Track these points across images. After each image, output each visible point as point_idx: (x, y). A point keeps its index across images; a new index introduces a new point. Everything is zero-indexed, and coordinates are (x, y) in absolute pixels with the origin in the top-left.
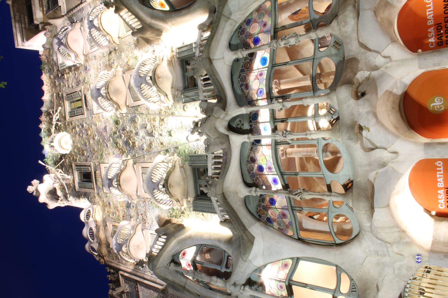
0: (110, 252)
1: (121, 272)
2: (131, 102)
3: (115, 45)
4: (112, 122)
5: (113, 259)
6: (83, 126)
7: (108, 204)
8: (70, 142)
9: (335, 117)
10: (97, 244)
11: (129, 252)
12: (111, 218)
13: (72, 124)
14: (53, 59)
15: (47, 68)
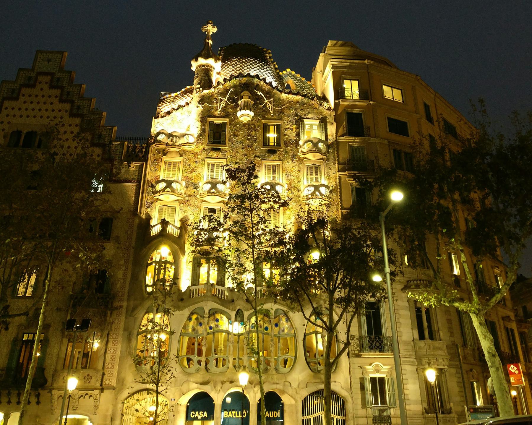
0: (159, 153)
8: (245, 122)
14: (309, 113)
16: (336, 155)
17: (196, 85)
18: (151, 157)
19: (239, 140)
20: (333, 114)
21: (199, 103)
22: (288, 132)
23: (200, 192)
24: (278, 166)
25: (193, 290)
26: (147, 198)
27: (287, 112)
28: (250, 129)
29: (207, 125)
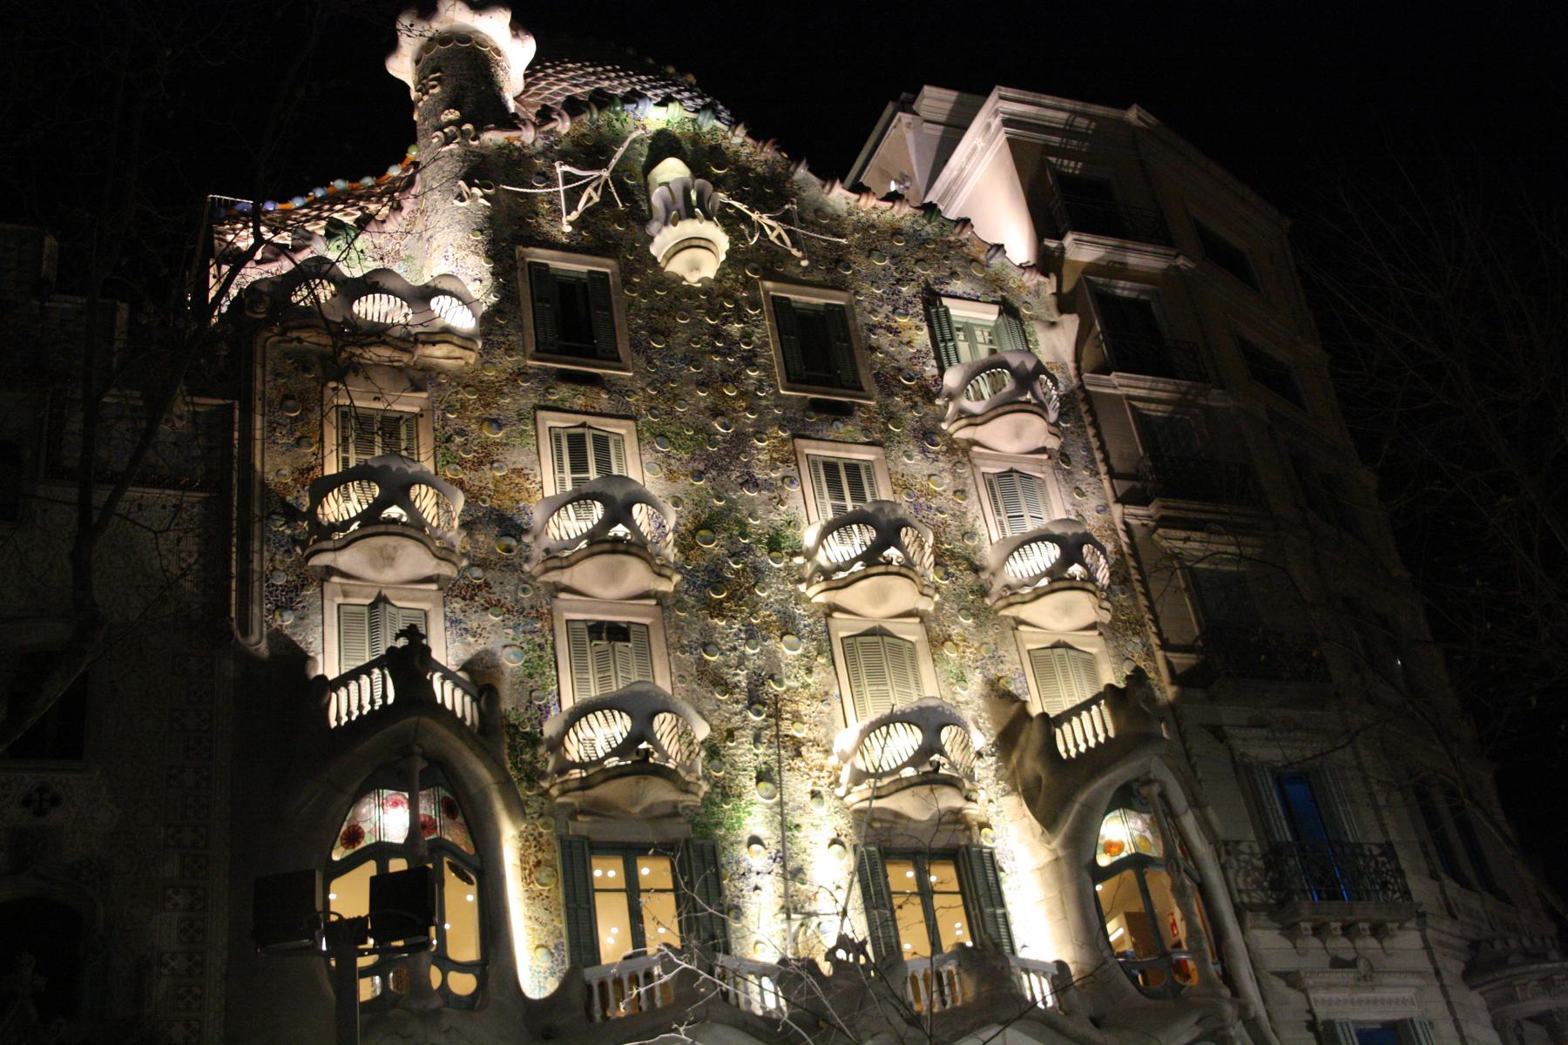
0: (306, 370)
2: (842, 627)
3: (1001, 603)
4: (775, 518)
6: (749, 360)
7: (494, 413)
8: (693, 279)
10: (339, 320)
11: (382, 528)
12: (445, 419)
13: (754, 306)
14: (953, 274)
15: (928, 228)
16: (1095, 443)
19: (679, 352)
20: (1049, 286)
22: (883, 339)
24: (869, 466)
26: (268, 565)
27: (861, 264)
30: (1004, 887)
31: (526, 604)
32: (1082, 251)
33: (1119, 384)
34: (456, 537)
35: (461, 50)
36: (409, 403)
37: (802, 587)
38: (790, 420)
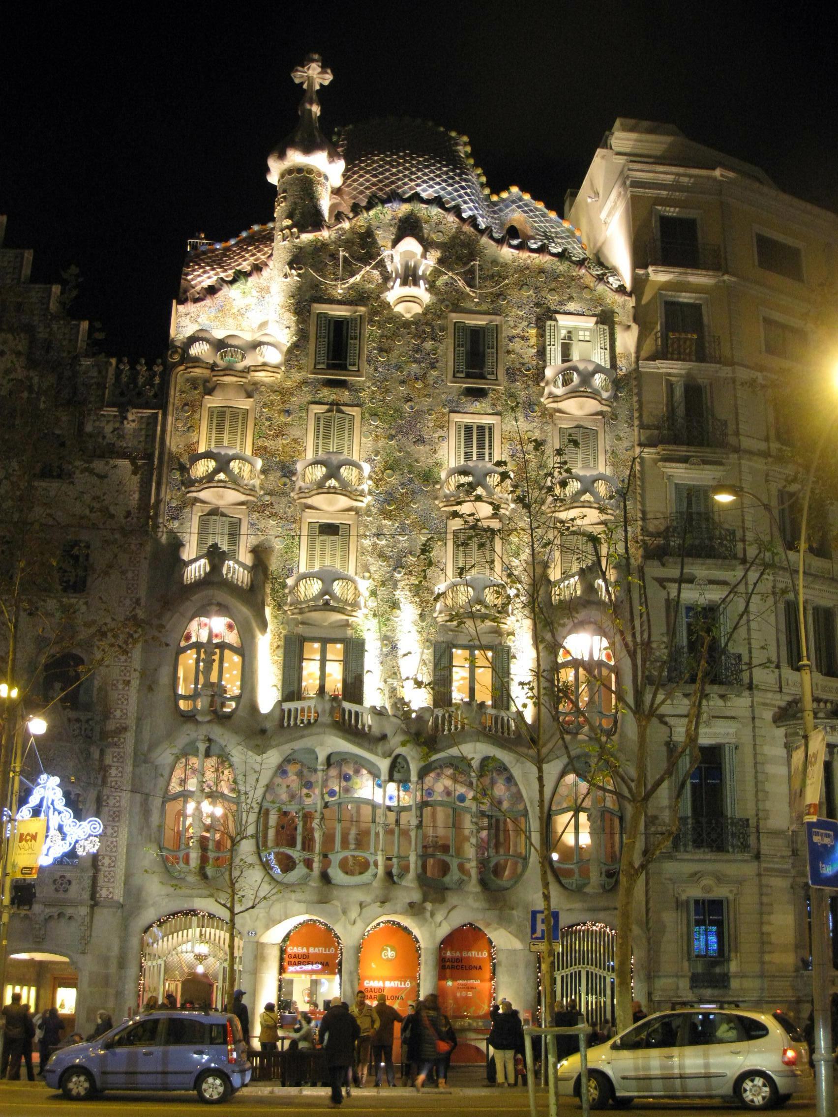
0: (196, 388)
1: (160, 416)
5: (183, 392)
6: (433, 366)
7: (287, 407)
8: (408, 316)
9: (395, 878)
14: (571, 298)
16: (636, 406)
17: (281, 219)
18: (175, 397)
19: (394, 361)
20: (631, 302)
21: (290, 264)
22: (517, 345)
23: (300, 483)
24: (491, 428)
25: (290, 711)
26: (168, 497)
27: (515, 295)
28: (421, 336)
29: (313, 320)
30: (512, 666)
31: (289, 515)
32: (659, 276)
33: (662, 367)
34: (257, 482)
35: (297, 179)
36: (245, 404)
37: (437, 502)
38: (451, 401)
